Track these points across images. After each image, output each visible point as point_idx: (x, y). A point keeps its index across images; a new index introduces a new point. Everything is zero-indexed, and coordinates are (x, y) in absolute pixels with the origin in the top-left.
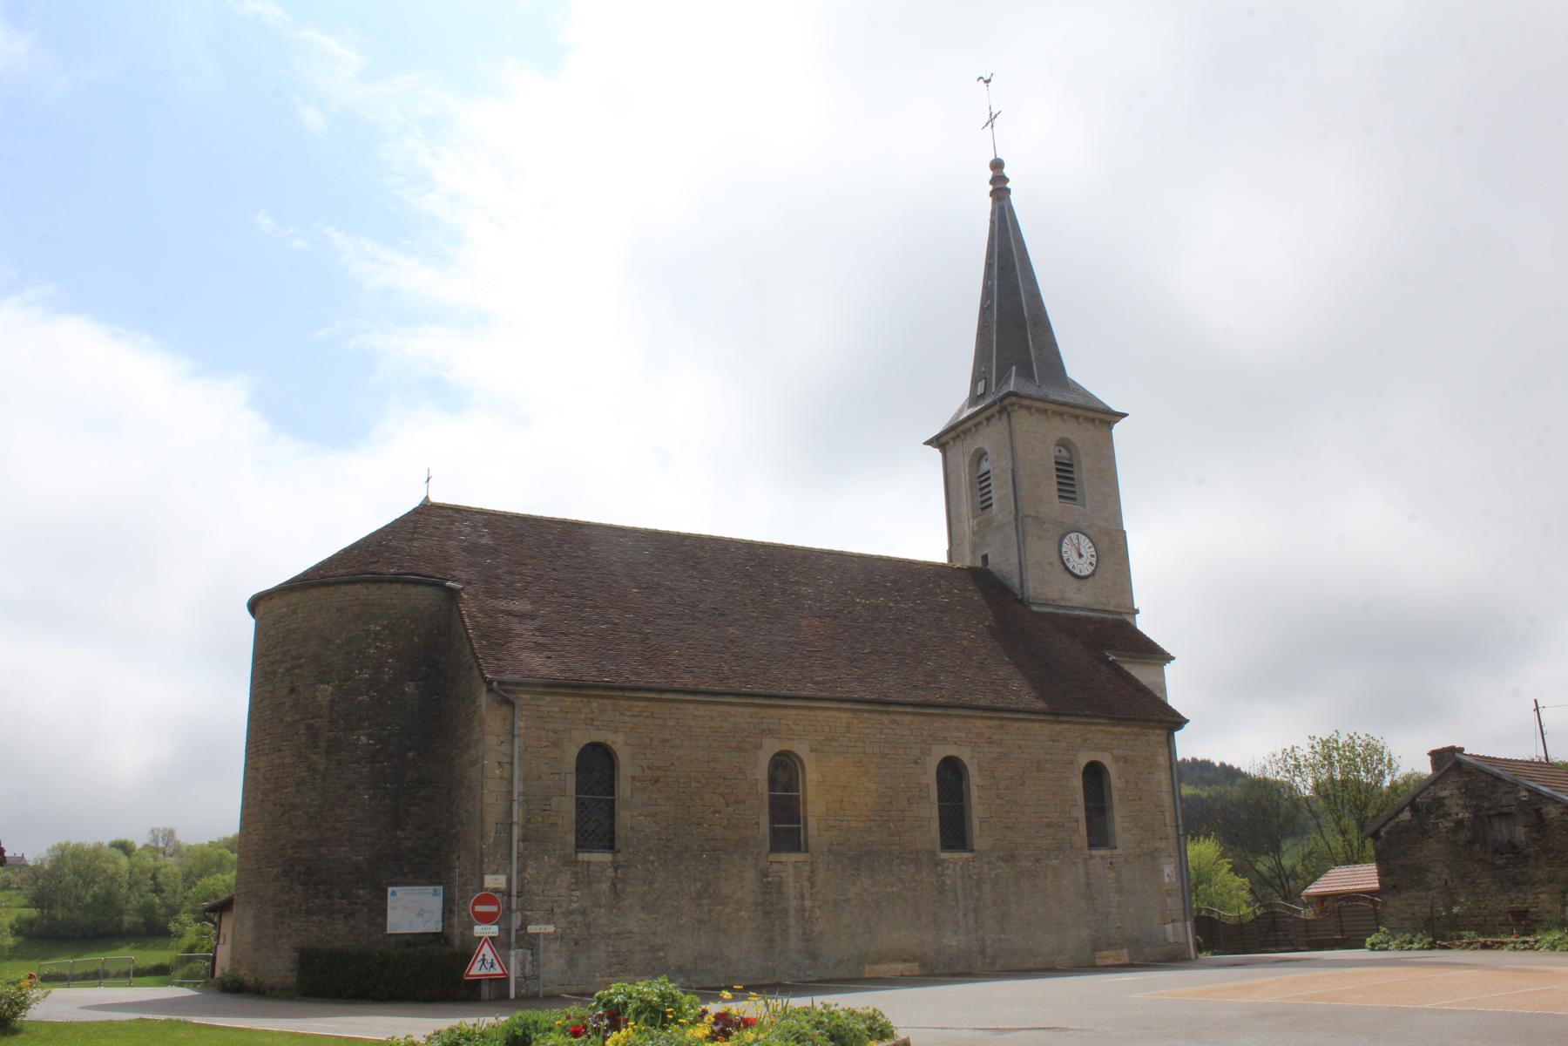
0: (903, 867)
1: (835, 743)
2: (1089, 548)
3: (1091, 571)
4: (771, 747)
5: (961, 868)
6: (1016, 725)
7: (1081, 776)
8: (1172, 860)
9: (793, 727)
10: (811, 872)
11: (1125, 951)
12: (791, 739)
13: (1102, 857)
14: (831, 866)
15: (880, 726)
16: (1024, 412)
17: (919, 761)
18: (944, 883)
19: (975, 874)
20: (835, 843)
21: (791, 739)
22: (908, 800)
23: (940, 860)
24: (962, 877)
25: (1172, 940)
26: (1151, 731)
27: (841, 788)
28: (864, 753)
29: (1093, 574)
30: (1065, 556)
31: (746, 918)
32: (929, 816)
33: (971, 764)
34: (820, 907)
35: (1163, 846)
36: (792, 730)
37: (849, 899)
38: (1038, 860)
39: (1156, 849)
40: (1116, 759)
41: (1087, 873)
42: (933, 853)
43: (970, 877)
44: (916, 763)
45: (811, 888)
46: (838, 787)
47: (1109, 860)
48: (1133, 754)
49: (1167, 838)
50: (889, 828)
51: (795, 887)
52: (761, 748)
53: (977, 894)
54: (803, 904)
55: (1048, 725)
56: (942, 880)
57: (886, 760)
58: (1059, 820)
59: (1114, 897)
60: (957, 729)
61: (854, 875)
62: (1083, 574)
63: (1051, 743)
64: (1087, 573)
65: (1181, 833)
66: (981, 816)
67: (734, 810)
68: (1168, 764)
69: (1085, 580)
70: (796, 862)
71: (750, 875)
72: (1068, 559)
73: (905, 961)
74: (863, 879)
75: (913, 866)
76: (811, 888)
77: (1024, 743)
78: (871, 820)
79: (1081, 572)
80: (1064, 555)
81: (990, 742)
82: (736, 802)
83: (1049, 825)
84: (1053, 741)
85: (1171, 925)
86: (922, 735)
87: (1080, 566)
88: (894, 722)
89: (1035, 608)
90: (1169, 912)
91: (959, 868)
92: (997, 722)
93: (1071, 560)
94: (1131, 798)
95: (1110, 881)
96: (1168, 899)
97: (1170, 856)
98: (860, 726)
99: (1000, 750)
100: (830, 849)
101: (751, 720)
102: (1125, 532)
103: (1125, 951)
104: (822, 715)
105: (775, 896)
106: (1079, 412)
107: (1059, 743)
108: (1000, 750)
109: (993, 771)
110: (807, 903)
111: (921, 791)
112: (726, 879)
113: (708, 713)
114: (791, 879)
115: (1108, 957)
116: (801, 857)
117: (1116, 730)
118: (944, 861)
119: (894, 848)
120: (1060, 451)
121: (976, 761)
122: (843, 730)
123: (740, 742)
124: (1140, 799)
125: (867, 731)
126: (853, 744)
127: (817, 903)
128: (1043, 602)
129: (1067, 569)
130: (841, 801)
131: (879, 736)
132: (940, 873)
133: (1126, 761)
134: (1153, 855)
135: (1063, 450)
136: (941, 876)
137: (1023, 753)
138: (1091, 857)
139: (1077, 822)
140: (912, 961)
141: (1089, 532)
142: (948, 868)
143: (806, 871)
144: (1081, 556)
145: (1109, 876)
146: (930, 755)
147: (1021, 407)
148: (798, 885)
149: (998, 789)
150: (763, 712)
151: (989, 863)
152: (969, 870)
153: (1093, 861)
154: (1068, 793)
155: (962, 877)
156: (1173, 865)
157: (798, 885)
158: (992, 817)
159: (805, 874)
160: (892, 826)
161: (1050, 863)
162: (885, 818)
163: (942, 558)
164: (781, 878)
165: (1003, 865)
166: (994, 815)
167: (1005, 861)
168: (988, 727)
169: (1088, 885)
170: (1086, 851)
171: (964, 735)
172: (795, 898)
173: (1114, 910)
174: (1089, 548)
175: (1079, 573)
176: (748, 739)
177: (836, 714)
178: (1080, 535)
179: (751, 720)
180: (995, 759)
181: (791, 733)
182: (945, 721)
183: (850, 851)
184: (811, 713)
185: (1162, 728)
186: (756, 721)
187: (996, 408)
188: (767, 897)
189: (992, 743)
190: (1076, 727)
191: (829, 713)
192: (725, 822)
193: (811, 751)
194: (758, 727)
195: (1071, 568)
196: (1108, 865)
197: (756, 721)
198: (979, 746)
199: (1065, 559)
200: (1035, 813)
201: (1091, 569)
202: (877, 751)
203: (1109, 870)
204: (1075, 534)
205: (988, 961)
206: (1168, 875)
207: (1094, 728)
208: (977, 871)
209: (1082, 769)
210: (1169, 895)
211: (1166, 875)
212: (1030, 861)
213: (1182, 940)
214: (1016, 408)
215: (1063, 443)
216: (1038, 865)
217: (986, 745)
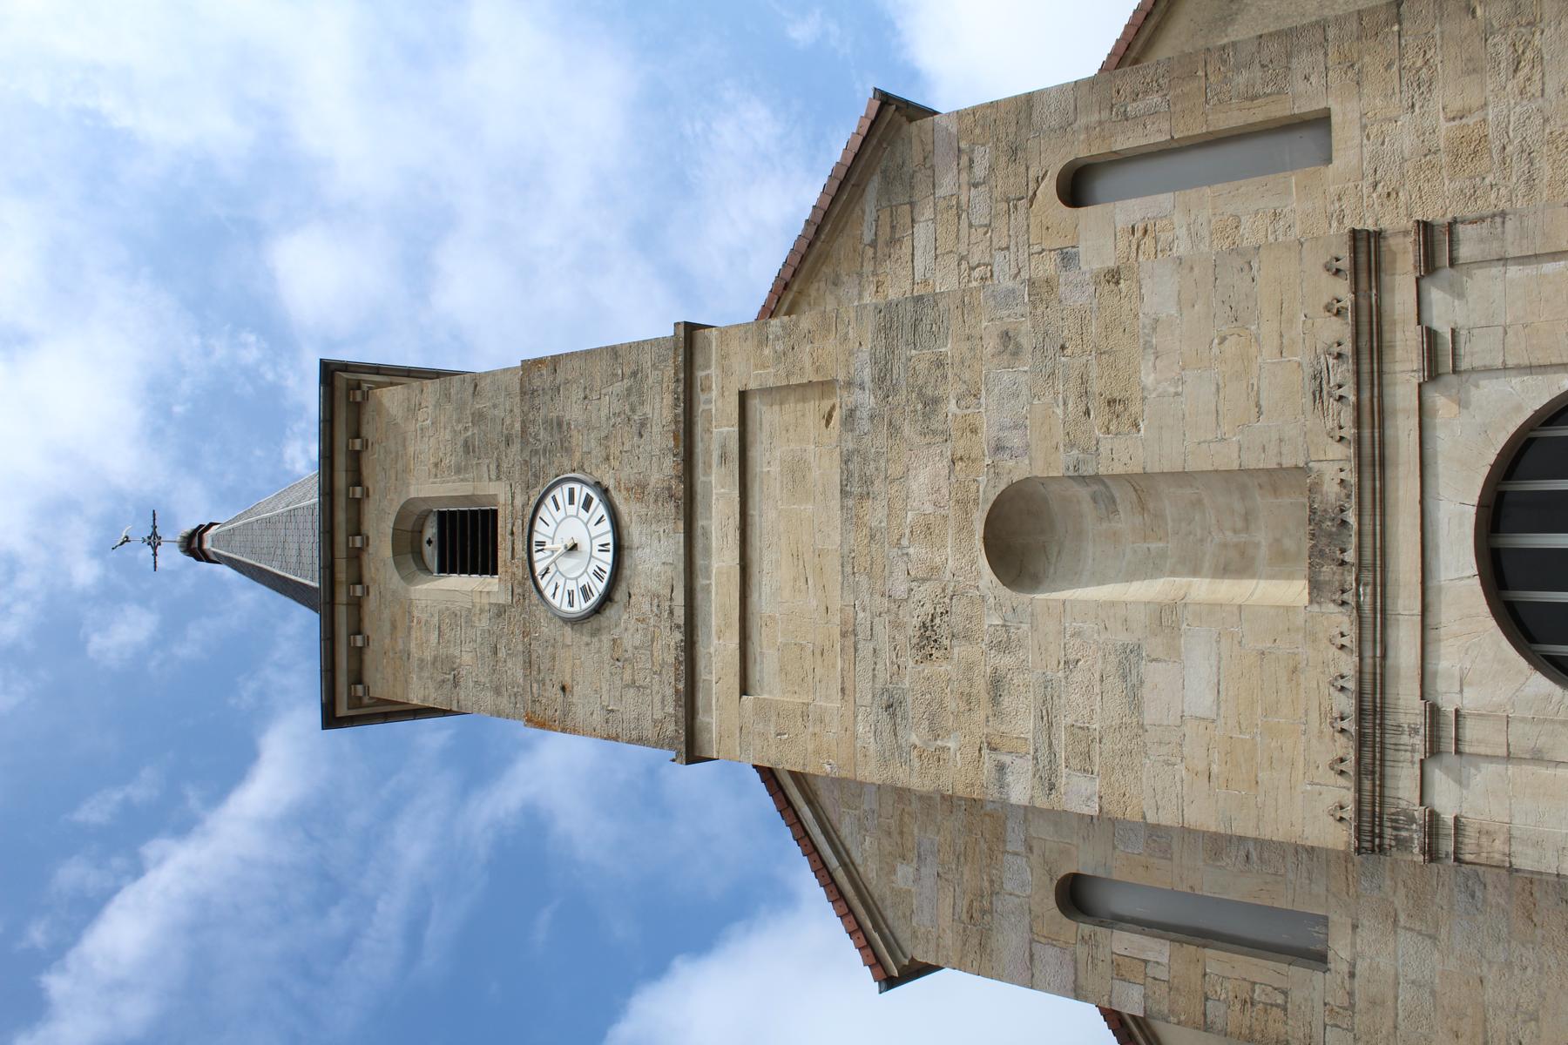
30: (581, 606)
62: (609, 539)
64: (606, 525)
72: (586, 592)
80: (576, 608)
87: (596, 553)
93: (583, 581)
129: (607, 598)
147: (357, 677)
175: (608, 557)
199: (585, 606)
215: (407, 546)
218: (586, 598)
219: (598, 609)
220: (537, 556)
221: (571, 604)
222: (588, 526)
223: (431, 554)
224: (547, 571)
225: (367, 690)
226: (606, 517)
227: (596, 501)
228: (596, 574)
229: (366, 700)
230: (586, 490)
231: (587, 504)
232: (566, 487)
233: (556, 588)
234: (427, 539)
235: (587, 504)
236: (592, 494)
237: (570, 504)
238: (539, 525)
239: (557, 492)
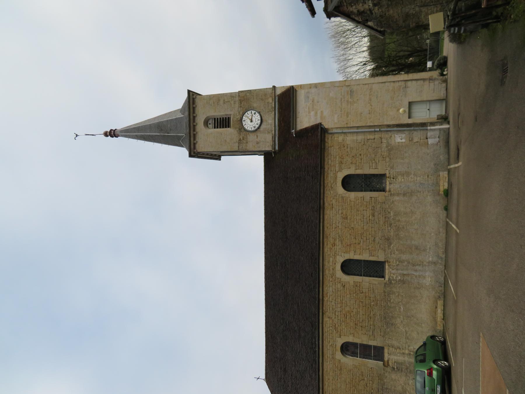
0: (392, 301)
1: (337, 326)
2: (248, 114)
4: (339, 355)
5: (393, 270)
6: (326, 229)
7: (349, 193)
8: (393, 136)
9: (331, 344)
10: (393, 347)
11: (441, 173)
12: (336, 346)
13: (390, 184)
14: (390, 337)
15: (329, 302)
16: (197, 146)
17: (343, 285)
18: (400, 280)
19: (396, 262)
20: (380, 333)
21: (336, 346)
22: (361, 293)
23: (389, 280)
24: (397, 270)
25: (437, 139)
26: (326, 144)
27: (356, 326)
28: (341, 312)
29: (259, 113)
30: (253, 129)
31: (412, 382)
32: (368, 284)
33: (344, 257)
34: (409, 346)
35: (386, 141)
36: (332, 344)
37: (406, 331)
38: (391, 225)
39: (387, 147)
40: (341, 170)
41: (398, 194)
42: (385, 284)
43: (398, 265)
44: (344, 286)
45: (400, 349)
46: (355, 328)
47: (392, 179)
48: (338, 157)
49: (381, 138)
50: (373, 305)
51: (399, 356)
52: (340, 360)
53: (406, 263)
54: (407, 354)
55: (325, 210)
56: (399, 281)
57: (344, 302)
58: (371, 209)
59: (411, 178)
60: (329, 262)
61: (395, 327)
62: (260, 119)
63: (333, 209)
64: (259, 116)
65: (378, 129)
66: (368, 255)
67: (366, 377)
68: (343, 135)
69: (262, 117)
70: (388, 353)
71: (393, 376)
72: (254, 127)
73: (436, 308)
74: (397, 322)
75: (391, 296)
76: (400, 349)
77: (334, 225)
78: (370, 314)
80: (253, 129)
81: (334, 245)
82: (362, 376)
83: (373, 215)
84: (332, 208)
85: (429, 140)
86: (332, 281)
88: (327, 294)
89: (277, 148)
90: (421, 140)
91: (393, 271)
92: (325, 240)
93: (254, 125)
94: (360, 161)
95: (403, 180)
96: (414, 141)
97: (391, 137)
98: (329, 312)
99: (338, 240)
100: (383, 336)
101: (329, 362)
102: (239, 91)
103: (441, 173)
104: (325, 330)
105: (403, 366)
106: (192, 117)
107: (334, 205)
108: (338, 240)
109: (347, 245)
110: (407, 352)
111: (357, 286)
112: (395, 387)
113: (327, 380)
114: (396, 358)
115: (444, 186)
116: (386, 351)
117: (326, 170)
118: (389, 279)
119: (382, 305)
120: (210, 124)
121: (343, 254)
122: (331, 321)
123: (338, 368)
124: (361, 155)
125: (331, 308)
126: (337, 316)
127: (407, 347)
128: (274, 143)
129: (259, 128)
130: (362, 327)
131: (333, 303)
132: (395, 281)
133: (341, 162)
134: (390, 149)
135: (209, 123)
136: (396, 282)
137: (338, 226)
138: (390, 191)
139: (372, 197)
140: (437, 303)
141: (241, 113)
142: (393, 277)
143: (392, 350)
144: (251, 121)
145: (400, 180)
146: (341, 279)
147: (195, 148)
148: (398, 355)
149: (356, 244)
150: (325, 357)
151: (391, 254)
152: (394, 266)
153: (392, 190)
154: (357, 201)
155: (397, 270)
156: (396, 135)
157: (398, 355)
158: (369, 248)
159: (393, 351)
160: (372, 304)
161: (392, 217)
162: (369, 307)
163: (263, 156)
164: (395, 362)
165: (392, 245)
166: (368, 248)
167: (391, 244)
168: (327, 245)
169: (404, 195)
170: (387, 194)
171: (331, 259)
172: (404, 357)
173: (418, 178)
174: (248, 114)
175: (259, 121)
176: (337, 366)
177: (324, 323)
178: (243, 119)
179: (329, 362)
180: (342, 243)
181: (333, 345)
182: (325, 269)
183: (384, 327)
184: (325, 335)
185: (325, 137)
186: (329, 360)
187: (199, 155)
188: (403, 370)
189: (334, 244)
190: (326, 192)
191: (324, 326)
192: (371, 382)
193: (341, 337)
194: (331, 360)
195: (258, 126)
196: (394, 180)
197: (329, 360)
198: (336, 251)
199: (254, 129)
200: (367, 223)
202: (339, 305)
203: (397, 179)
204: (243, 122)
205: (440, 261)
206: (401, 139)
207: (326, 182)
208: (395, 261)
209: (346, 192)
210: (412, 140)
211: (401, 141)
212: (390, 229)
213: (437, 133)
214: (196, 151)
215: (206, 123)
216: (393, 225)
217: (335, 247)
218: (255, 128)
219: (256, 130)
221: (251, 129)
224: (246, 124)
227: (257, 113)
228: (257, 124)
231: (255, 113)
232: (250, 111)
233: (248, 127)
235: (255, 113)
237: (254, 114)
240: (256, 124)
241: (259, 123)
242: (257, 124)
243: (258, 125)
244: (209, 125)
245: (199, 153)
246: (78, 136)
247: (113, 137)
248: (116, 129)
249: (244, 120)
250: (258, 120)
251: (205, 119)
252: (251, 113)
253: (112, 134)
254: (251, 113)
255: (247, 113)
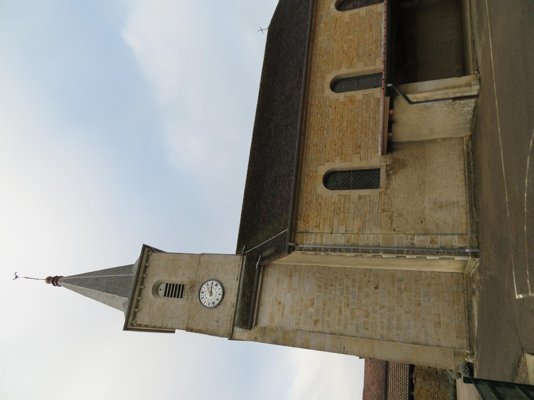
3: (220, 287)
29: (221, 284)
30: (211, 305)
62: (221, 293)
64: (221, 290)
72: (213, 303)
79: (220, 294)
80: (210, 306)
87: (217, 295)
93: (213, 301)
129: (219, 304)
175: (221, 296)
178: (201, 291)
195: (218, 302)
199: (212, 306)
201: (219, 286)
215: (156, 289)
220: (201, 295)
221: (209, 305)
222: (216, 290)
223: (162, 293)
225: (136, 322)
226: (221, 288)
227: (219, 285)
228: (217, 299)
229: (135, 325)
230: (216, 282)
231: (216, 285)
232: (211, 282)
234: (160, 289)
235: (216, 285)
236: (218, 283)
238: (202, 288)
239: (209, 282)
240: (215, 299)
241: (220, 299)
242: (217, 299)
243: (218, 301)
244: (159, 291)
245: (140, 325)
246: (18, 277)
247: (55, 286)
248: (61, 277)
249: (202, 292)
250: (220, 294)
251: (155, 283)
252: (212, 283)
253: (54, 281)
254: (212, 283)
255: (208, 284)
